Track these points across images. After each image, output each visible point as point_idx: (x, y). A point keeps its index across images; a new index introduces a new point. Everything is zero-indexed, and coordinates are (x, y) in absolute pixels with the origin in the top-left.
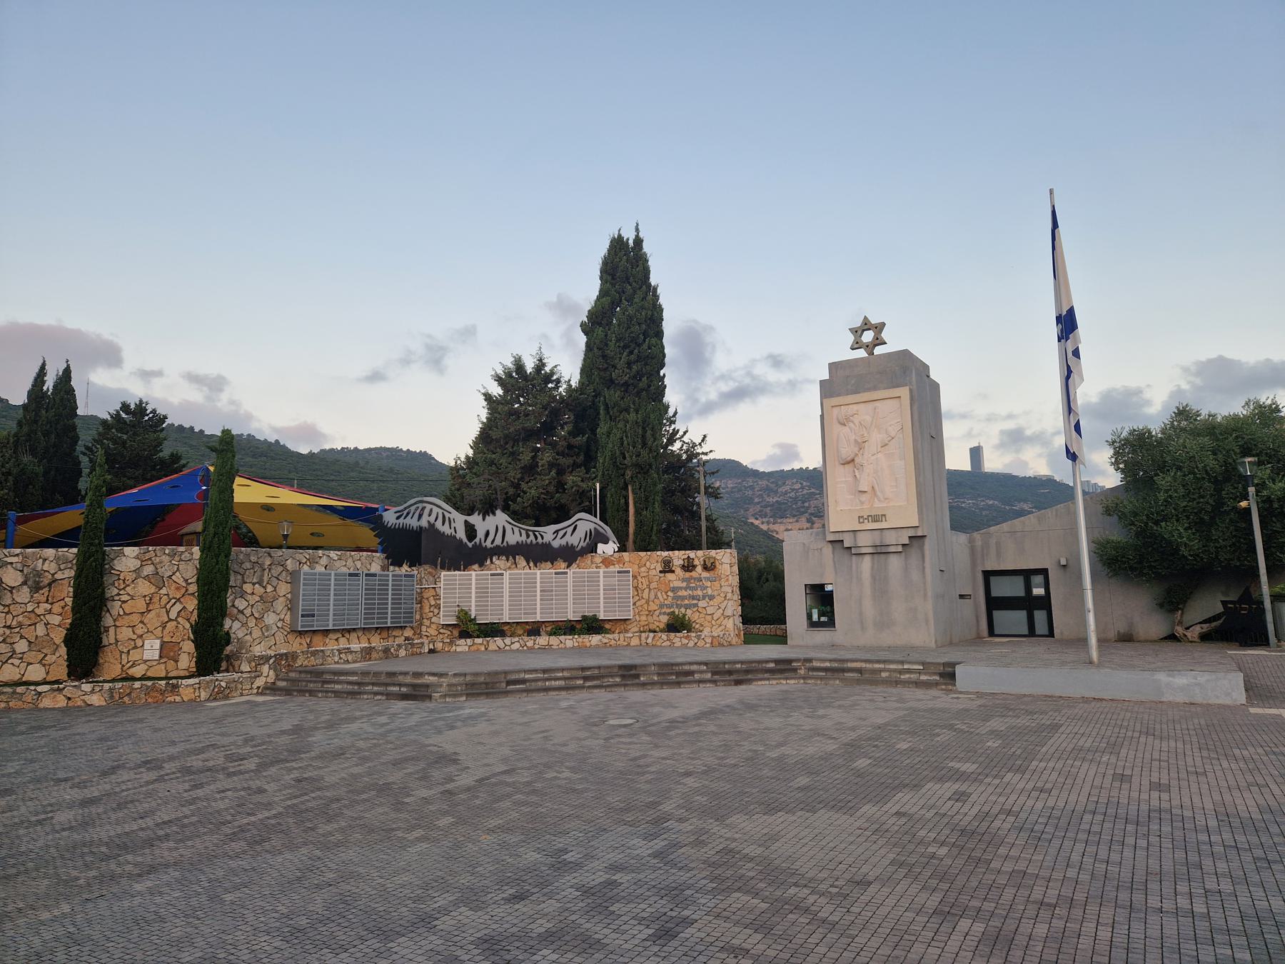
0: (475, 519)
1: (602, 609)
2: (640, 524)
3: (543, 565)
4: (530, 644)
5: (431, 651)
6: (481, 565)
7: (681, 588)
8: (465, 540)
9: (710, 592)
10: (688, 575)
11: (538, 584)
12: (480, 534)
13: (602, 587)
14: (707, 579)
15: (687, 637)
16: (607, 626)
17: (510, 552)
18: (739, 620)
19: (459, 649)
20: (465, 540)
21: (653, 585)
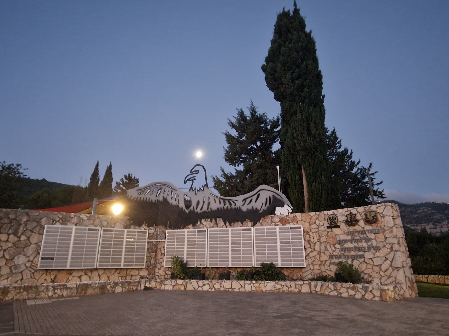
1: (279, 259)
2: (311, 193)
3: (236, 224)
4: (217, 286)
5: (146, 289)
6: (194, 225)
7: (346, 241)
8: (184, 208)
9: (374, 243)
10: (352, 229)
11: (230, 239)
12: (194, 204)
13: (278, 241)
14: (371, 231)
15: (353, 288)
16: (286, 273)
17: (212, 215)
18: (409, 272)
19: (167, 288)
20: (184, 208)
21: (323, 239)
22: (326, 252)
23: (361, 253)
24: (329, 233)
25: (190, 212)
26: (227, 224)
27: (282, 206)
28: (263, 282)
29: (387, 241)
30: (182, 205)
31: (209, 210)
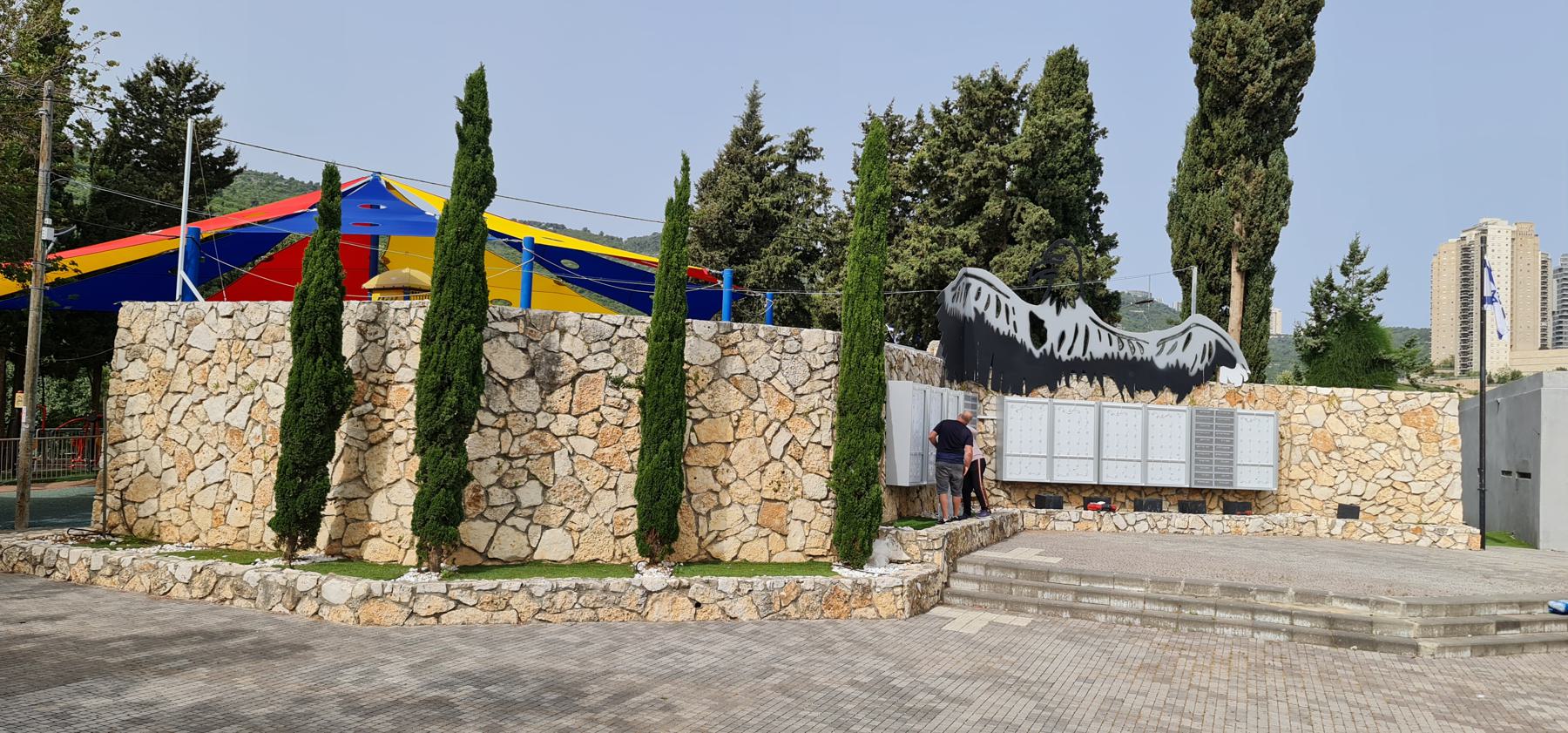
0: (1045, 311)
4: (1162, 524)
8: (1029, 345)
12: (1052, 338)
17: (1094, 369)
19: (1059, 526)
20: (1029, 345)
22: (1303, 464)
23: (1388, 472)
24: (1318, 431)
25: (1044, 355)
26: (1125, 392)
27: (1233, 366)
28: (1242, 517)
29: (1444, 456)
30: (1024, 335)
31: (1088, 356)
